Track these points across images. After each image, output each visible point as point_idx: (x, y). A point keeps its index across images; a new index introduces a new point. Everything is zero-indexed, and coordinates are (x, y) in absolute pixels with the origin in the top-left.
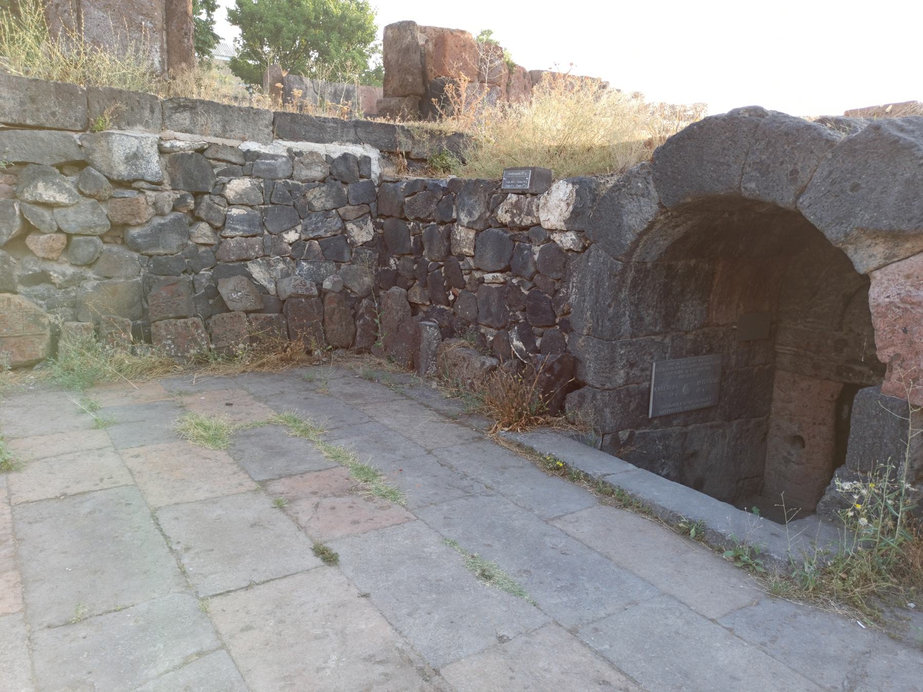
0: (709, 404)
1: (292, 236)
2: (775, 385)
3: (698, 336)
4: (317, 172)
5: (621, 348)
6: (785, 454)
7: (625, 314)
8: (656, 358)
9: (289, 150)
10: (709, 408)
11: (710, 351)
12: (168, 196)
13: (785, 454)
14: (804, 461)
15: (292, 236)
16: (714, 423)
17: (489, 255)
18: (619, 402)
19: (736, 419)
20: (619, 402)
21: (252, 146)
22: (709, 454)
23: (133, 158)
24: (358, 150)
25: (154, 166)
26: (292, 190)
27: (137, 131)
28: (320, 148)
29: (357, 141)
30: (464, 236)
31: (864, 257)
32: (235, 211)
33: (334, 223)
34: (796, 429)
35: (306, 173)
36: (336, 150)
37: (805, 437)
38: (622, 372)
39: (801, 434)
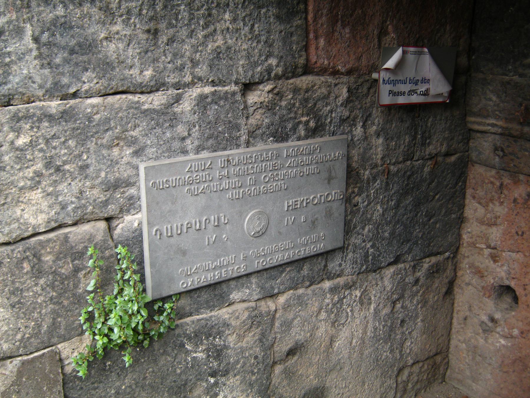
0: (321, 247)
2: (469, 192)
3: (280, 95)
5: (18, 132)
6: (485, 318)
7: (19, 32)
8: (151, 151)
10: (327, 254)
11: (313, 133)
13: (485, 318)
14: (516, 332)
16: (341, 281)
18: (38, 272)
19: (390, 264)
20: (38, 272)
22: (332, 341)
34: (503, 274)
37: (519, 291)
38: (36, 195)
39: (512, 284)
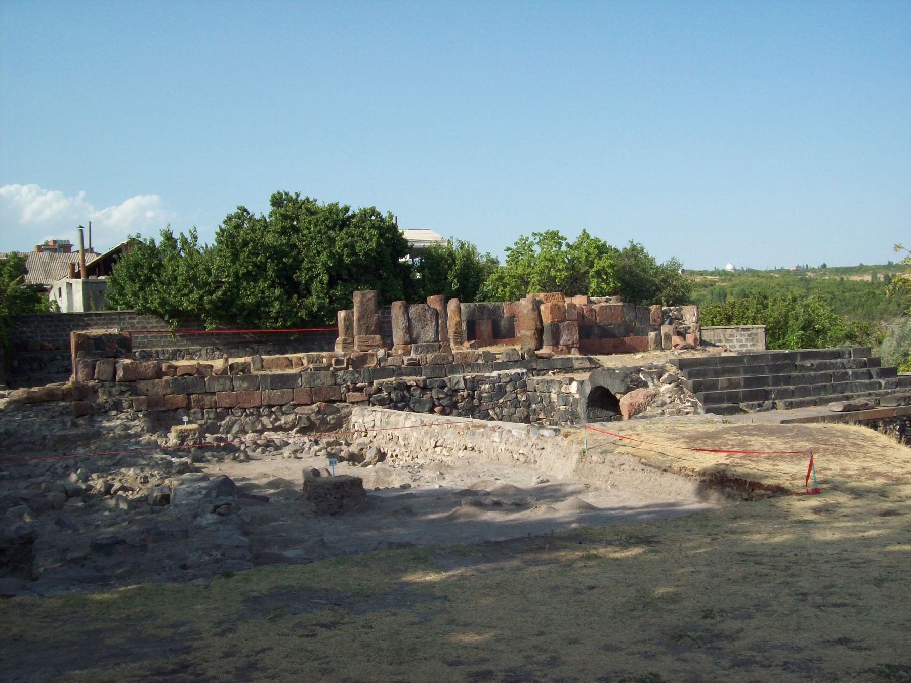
1: (501, 401)
4: (508, 379)
9: (499, 375)
12: (465, 393)
15: (501, 401)
17: (561, 401)
21: (487, 374)
23: (458, 383)
24: (519, 371)
25: (462, 385)
26: (500, 386)
27: (457, 376)
28: (507, 372)
29: (518, 368)
30: (554, 396)
31: (618, 396)
32: (485, 395)
33: (514, 395)
35: (503, 380)
36: (513, 371)
